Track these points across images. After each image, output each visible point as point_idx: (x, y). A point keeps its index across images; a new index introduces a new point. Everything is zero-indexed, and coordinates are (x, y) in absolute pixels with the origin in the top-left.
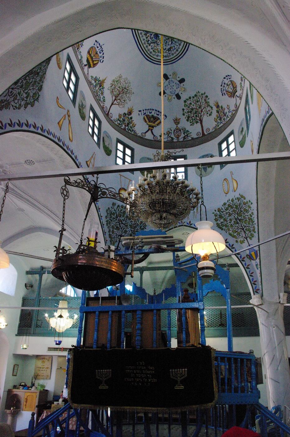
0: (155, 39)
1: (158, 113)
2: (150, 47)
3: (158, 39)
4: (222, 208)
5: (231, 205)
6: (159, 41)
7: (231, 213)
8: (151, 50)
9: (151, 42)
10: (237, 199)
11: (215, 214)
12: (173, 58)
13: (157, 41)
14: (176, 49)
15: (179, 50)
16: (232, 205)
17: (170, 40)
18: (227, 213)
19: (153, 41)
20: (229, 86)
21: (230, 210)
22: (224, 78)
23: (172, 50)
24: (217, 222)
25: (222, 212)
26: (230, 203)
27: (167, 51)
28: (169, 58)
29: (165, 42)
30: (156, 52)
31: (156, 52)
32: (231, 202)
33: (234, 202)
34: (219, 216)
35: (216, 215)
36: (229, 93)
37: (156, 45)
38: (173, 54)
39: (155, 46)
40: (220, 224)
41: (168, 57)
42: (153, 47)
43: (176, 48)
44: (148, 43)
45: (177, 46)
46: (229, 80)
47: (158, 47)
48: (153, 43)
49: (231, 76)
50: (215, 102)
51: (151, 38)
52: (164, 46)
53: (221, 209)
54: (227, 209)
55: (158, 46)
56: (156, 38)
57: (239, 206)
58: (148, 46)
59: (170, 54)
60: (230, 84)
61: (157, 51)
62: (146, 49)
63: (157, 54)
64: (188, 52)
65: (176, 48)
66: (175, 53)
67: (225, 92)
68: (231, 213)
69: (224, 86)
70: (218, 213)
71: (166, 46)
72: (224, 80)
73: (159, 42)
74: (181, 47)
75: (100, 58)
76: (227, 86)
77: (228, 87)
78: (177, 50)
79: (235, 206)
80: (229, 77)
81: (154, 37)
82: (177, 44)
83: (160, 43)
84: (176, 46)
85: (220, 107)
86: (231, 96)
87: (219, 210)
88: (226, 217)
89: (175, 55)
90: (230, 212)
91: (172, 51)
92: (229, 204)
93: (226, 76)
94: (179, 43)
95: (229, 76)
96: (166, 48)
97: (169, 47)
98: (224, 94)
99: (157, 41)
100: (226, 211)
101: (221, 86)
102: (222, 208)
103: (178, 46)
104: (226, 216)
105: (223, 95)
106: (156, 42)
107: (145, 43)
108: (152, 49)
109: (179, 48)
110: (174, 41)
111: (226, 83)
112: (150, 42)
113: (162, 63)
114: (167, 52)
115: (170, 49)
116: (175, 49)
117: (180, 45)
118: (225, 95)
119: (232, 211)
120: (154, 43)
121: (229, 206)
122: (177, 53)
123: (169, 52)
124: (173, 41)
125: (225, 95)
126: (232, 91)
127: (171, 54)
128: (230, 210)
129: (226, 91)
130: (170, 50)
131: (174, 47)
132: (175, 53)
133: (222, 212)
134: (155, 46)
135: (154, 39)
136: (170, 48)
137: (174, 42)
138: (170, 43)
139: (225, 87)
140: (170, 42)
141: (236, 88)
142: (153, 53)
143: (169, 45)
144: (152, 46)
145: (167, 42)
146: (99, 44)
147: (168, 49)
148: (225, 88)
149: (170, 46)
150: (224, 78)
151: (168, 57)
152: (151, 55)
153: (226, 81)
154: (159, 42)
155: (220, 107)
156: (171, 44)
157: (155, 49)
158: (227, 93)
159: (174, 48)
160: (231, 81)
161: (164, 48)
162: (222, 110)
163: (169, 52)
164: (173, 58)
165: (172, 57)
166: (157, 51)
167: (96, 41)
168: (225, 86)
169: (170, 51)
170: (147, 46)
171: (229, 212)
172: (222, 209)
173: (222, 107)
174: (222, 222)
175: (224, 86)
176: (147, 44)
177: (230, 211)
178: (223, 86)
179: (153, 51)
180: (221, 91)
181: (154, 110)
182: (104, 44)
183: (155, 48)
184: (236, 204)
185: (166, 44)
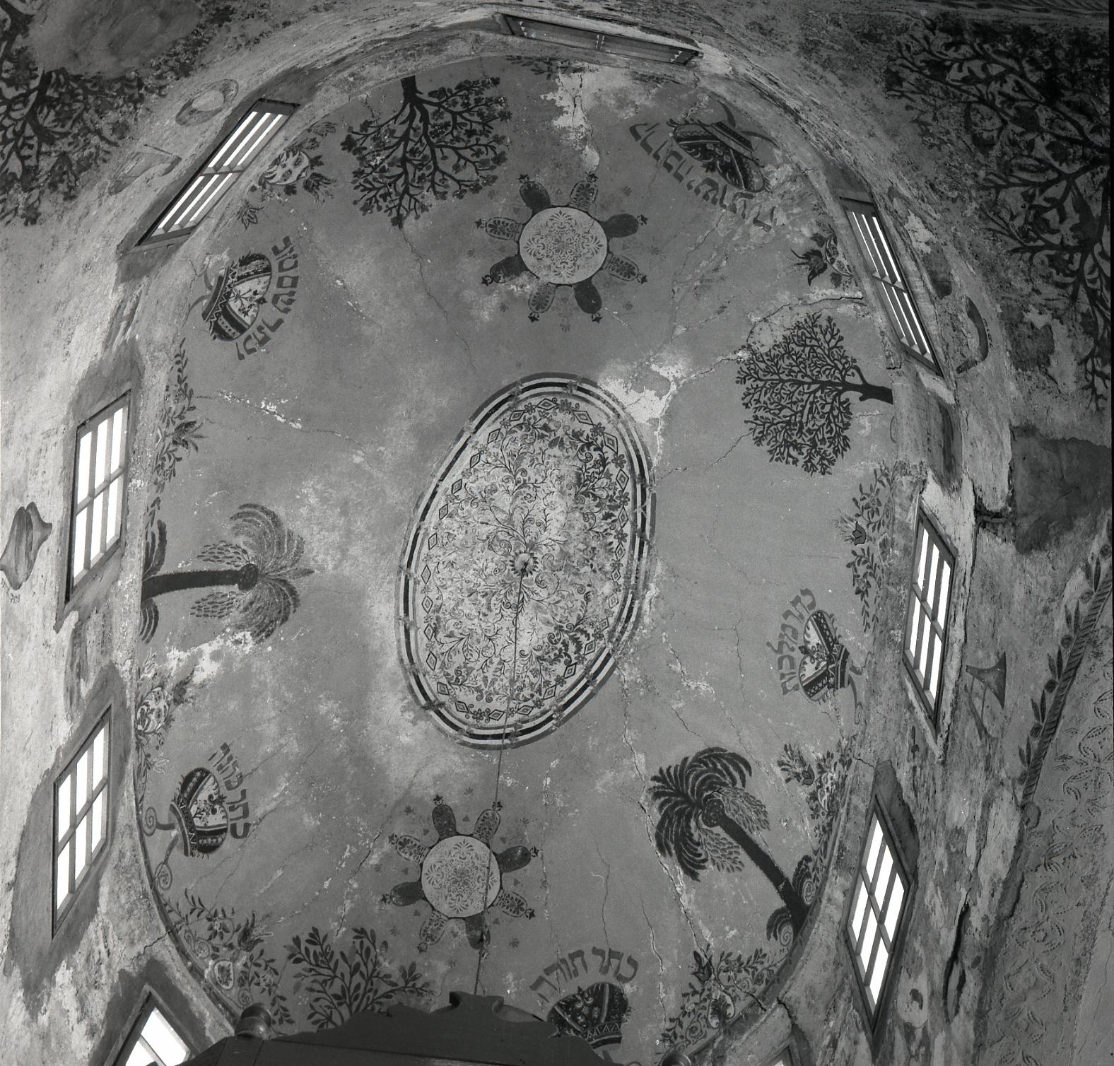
1: (672, 161)
22: (280, 322)
46: (253, 330)
98: (281, 246)
101: (295, 281)
111: (269, 305)
118: (276, 251)
139: (275, 280)
148: (276, 273)
150: (280, 322)
167: (785, 691)
175: (280, 285)
178: (287, 282)
181: (685, 181)
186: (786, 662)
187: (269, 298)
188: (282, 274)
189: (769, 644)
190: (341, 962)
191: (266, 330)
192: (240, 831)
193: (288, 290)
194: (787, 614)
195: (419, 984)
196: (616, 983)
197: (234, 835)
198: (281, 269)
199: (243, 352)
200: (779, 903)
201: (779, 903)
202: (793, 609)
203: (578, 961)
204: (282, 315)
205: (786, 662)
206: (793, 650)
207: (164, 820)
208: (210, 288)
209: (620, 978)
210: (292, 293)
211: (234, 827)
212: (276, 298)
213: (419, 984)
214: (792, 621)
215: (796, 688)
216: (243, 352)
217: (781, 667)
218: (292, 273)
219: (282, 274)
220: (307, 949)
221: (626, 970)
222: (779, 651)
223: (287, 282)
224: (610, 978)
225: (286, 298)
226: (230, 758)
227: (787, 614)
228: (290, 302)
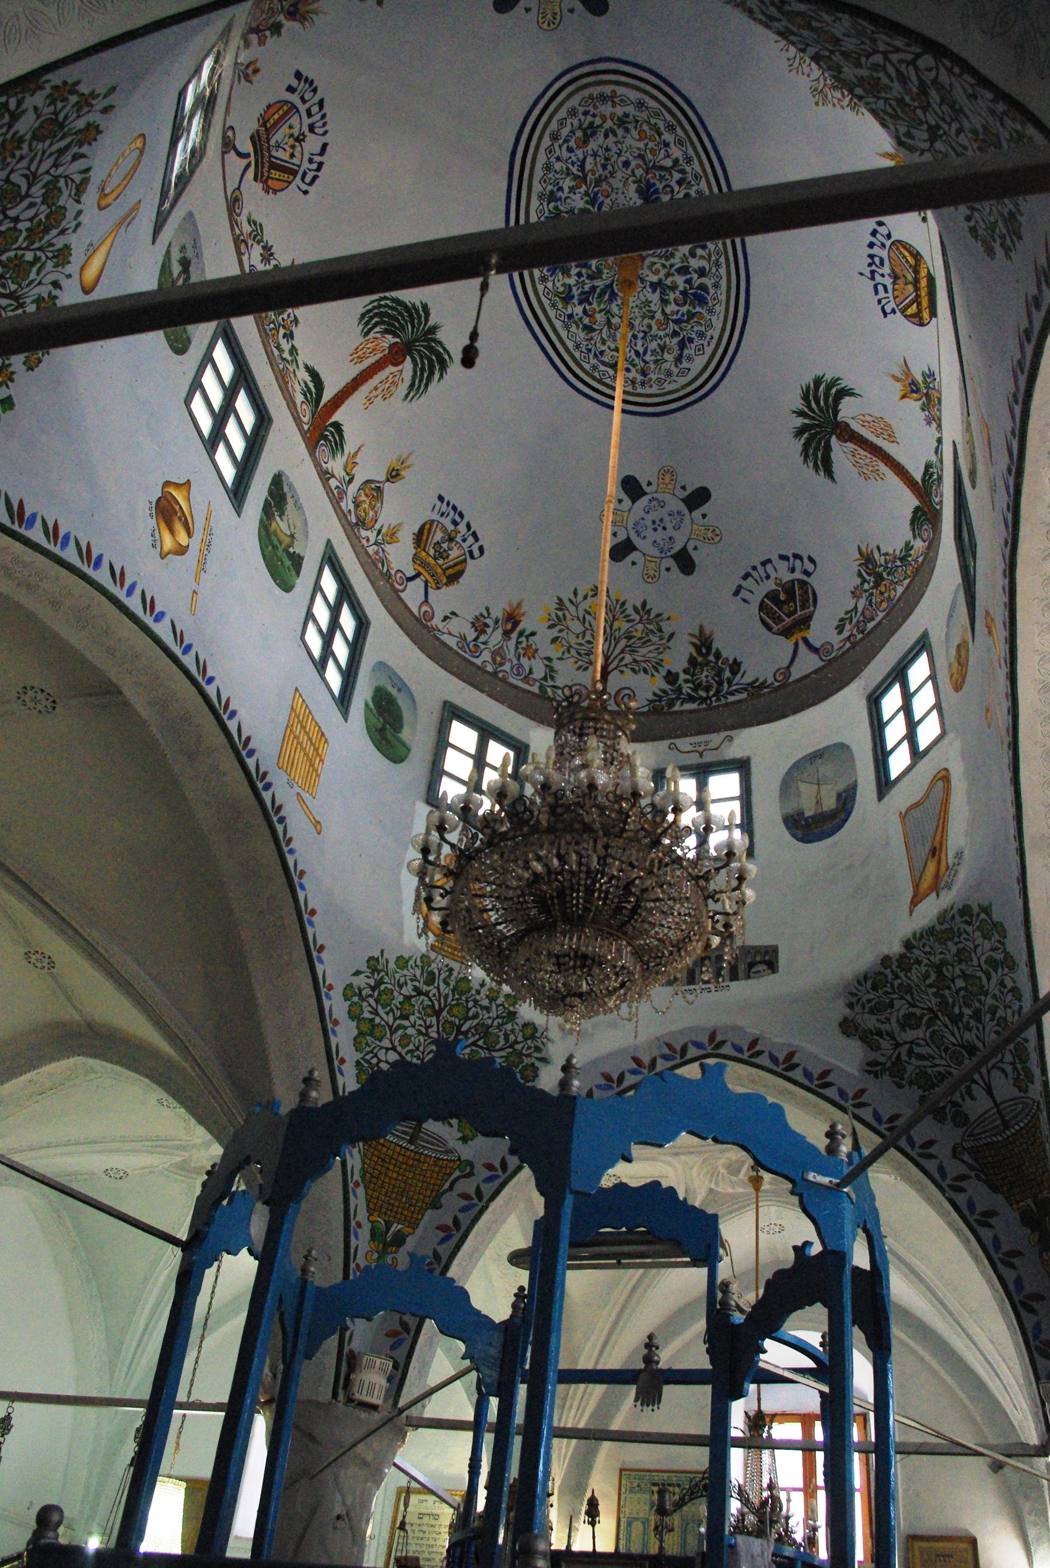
0: (652, 181)
2: (676, 152)
3: (640, 181)
4: (83, 156)
5: (54, 232)
6: (639, 172)
7: (12, 213)
8: (667, 137)
9: (671, 175)
10: (55, 292)
11: (98, 95)
12: (571, 95)
13: (647, 173)
14: (561, 142)
15: (546, 142)
16: (47, 238)
17: (590, 176)
18: (32, 178)
19: (662, 178)
20: (291, 141)
21: (31, 213)
22: (324, 146)
23: (579, 134)
24: (48, 90)
25: (61, 152)
26: (63, 232)
27: (601, 126)
28: (586, 93)
29: (609, 167)
30: (649, 123)
31: (649, 123)
32: (59, 243)
33: (50, 265)
34: (66, 117)
35: (86, 102)
36: (276, 117)
37: (650, 156)
38: (573, 113)
39: (652, 151)
40: (19, 103)
41: (591, 97)
42: (663, 152)
43: (560, 147)
44: (682, 172)
45: (558, 159)
46: (306, 165)
47: (641, 145)
48: (662, 168)
49: (306, 192)
50: (315, 12)
51: (672, 191)
52: (614, 149)
53: (85, 149)
54: (51, 191)
55: (638, 149)
56: (649, 185)
57: (13, 287)
58: (681, 162)
59: (586, 113)
60: (292, 156)
61: (645, 127)
62: (691, 152)
63: (643, 115)
64: (510, 149)
65: (560, 147)
66: (562, 123)
67: (295, 98)
68: (12, 213)
69: (309, 114)
70: (81, 124)
71: (608, 150)
72: (324, 139)
73: (638, 166)
74: (542, 158)
75: (888, 243)
76: (296, 135)
77: (291, 136)
78: (555, 137)
79: (29, 256)
80: (308, 179)
81: (656, 191)
82: (558, 166)
83: (633, 163)
84: (565, 154)
85: (284, 21)
86: (264, 125)
87: (91, 133)
88: (22, 158)
89: (562, 113)
90: (26, 202)
91: (576, 123)
92: (63, 224)
93: (320, 165)
94: (551, 176)
95: (315, 178)
96: (606, 136)
97: (592, 145)
98: (294, 83)
99: (647, 173)
100: (47, 178)
101: (321, 104)
102: (83, 156)
103: (553, 160)
104: (24, 163)
105: (298, 75)
106: (648, 169)
107: (696, 177)
108: (667, 145)
109: (550, 150)
110: (576, 178)
111: (310, 137)
112: (677, 176)
113: (618, 404)
114: (598, 121)
115: (585, 134)
116: (566, 141)
117: (548, 167)
118: (291, 89)
119: (16, 220)
120: (654, 167)
121: (57, 215)
122: (554, 125)
123: (589, 119)
124: (580, 174)
125: (291, 89)
126: (273, 142)
127: (581, 109)
128: (31, 213)
129: (294, 106)
130: (584, 131)
131: (570, 150)
132: (562, 123)
133: (61, 152)
134: (652, 151)
135: (660, 186)
136: (585, 142)
137: (574, 170)
138: (589, 165)
139: (304, 115)
140: (588, 166)
141: (265, 182)
142: (661, 125)
143: (595, 155)
144: (668, 156)
145: (604, 167)
146: (876, 292)
147: (594, 133)
148: (302, 108)
149: (589, 148)
150: (324, 146)
151: (591, 97)
152: (669, 118)
153: (312, 144)
154: (638, 166)
155: (284, 21)
156: (585, 158)
157: (651, 138)
158: (286, 102)
159: (572, 144)
160: (294, 173)
161: (612, 138)
162: (271, 22)
163: (589, 119)
164: (571, 95)
165: (574, 102)
166: (645, 127)
167: (885, 314)
168: (307, 121)
169: (585, 125)
170: (689, 160)
171: (27, 195)
172: (76, 157)
173: (276, 29)
174: (15, 117)
175: (309, 114)
176: (688, 169)
177: (32, 205)
178: (315, 109)
179: (660, 134)
180: (312, 83)
182: (861, 274)
183: (651, 145)
184: (33, 275)
185: (607, 159)
186: (880, 288)
187: (305, 129)
188: (307, 105)
189: (861, 274)
190: (588, 617)
191: (317, 159)
192: (476, 553)
193: (318, 117)
194: (871, 245)
195: (652, 615)
196: (805, 578)
197: (472, 557)
198: (304, 101)
199: (304, 187)
200: (916, 503)
201: (916, 503)
202: (874, 240)
203: (769, 567)
204: (324, 139)
205: (880, 288)
206: (883, 275)
207: (410, 573)
208: (247, 156)
209: (807, 573)
210: (324, 116)
211: (471, 553)
212: (312, 128)
213: (652, 615)
214: (875, 250)
215: (893, 311)
216: (304, 187)
217: (876, 292)
218: (316, 99)
219: (307, 105)
220: (557, 616)
221: (810, 567)
222: (873, 278)
223: (315, 109)
224: (798, 575)
225: (320, 124)
226: (448, 504)
227: (871, 245)
228: (325, 124)
